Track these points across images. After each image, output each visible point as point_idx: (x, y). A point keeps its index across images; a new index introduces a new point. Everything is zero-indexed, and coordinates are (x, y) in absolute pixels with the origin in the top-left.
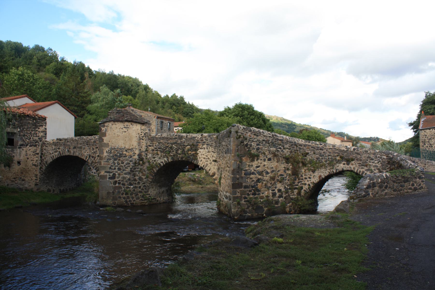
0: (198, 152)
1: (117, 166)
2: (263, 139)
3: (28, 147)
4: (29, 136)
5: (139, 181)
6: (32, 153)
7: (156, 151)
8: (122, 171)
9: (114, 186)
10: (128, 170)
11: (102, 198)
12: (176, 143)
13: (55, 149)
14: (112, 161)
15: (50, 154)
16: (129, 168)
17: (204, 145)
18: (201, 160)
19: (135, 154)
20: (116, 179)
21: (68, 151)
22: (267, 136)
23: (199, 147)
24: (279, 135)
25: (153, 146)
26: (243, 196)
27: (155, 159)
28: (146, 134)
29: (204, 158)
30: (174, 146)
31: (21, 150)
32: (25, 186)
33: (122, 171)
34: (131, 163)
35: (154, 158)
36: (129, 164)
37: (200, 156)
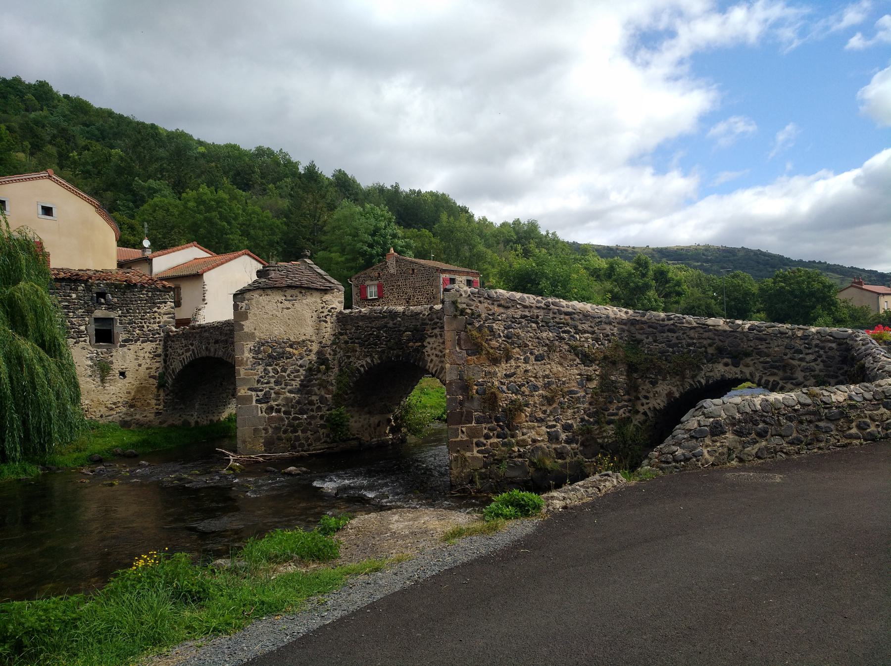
0: (425, 344)
1: (273, 377)
2: (524, 313)
3: (139, 343)
4: (141, 323)
5: (319, 404)
6: (147, 354)
7: (351, 343)
8: (283, 386)
9: (267, 416)
10: (296, 384)
11: (244, 442)
12: (386, 326)
13: (186, 346)
14: (260, 368)
15: (179, 355)
16: (298, 379)
17: (436, 328)
18: (432, 361)
19: (311, 351)
20: (273, 403)
21: (207, 348)
22: (531, 307)
23: (427, 334)
24: (564, 303)
25: (346, 334)
26: (475, 440)
27: (351, 360)
28: (333, 310)
29: (437, 356)
30: (382, 332)
31: (125, 349)
32: (135, 417)
33: (283, 386)
34: (301, 370)
35: (349, 357)
36: (298, 371)
37: (430, 352)
